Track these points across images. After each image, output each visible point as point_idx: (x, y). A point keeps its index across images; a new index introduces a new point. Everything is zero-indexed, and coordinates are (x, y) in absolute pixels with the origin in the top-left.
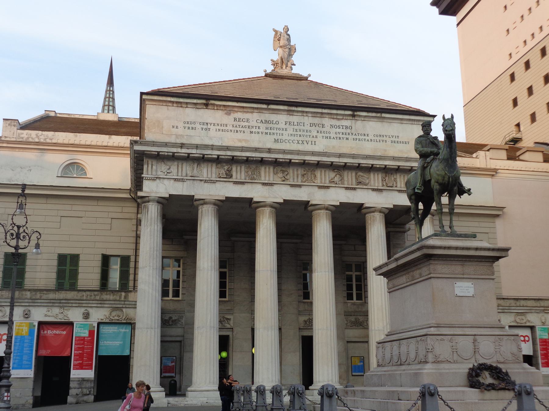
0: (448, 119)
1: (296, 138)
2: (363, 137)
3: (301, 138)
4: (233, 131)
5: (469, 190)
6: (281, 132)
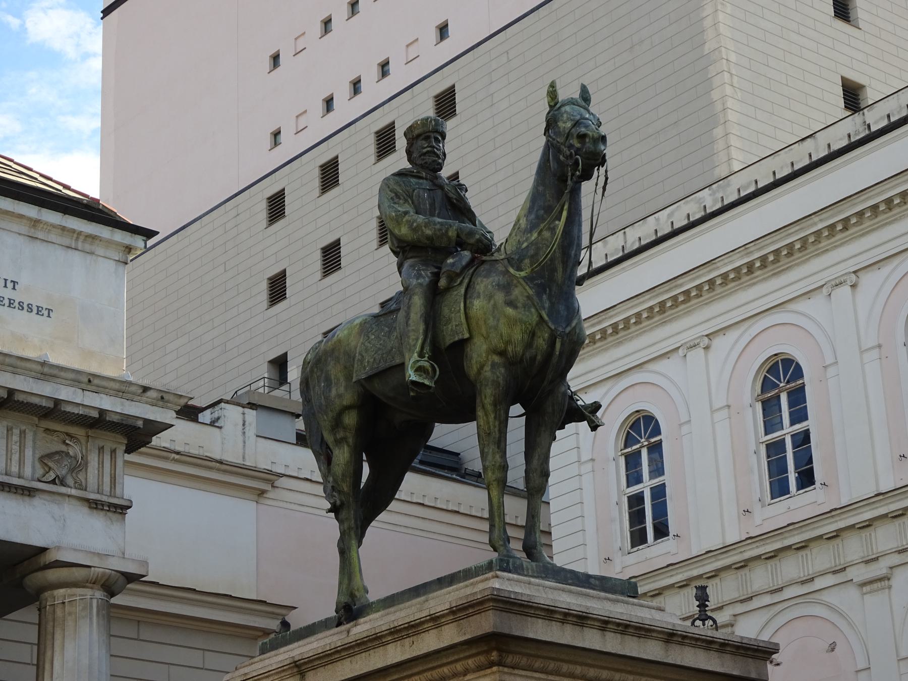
0: (572, 102)
5: (596, 406)
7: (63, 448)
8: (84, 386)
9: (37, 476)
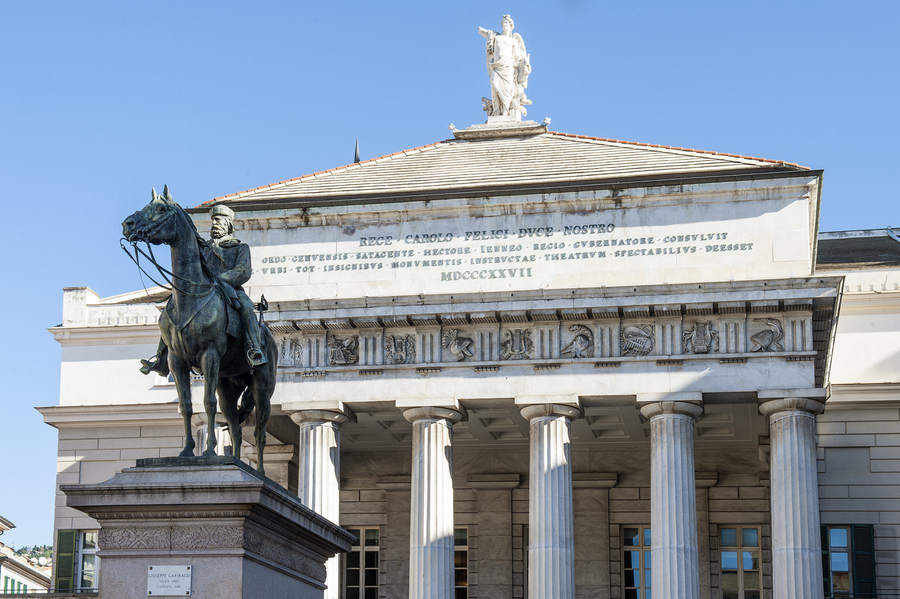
1: (488, 266)
2: (640, 246)
3: (501, 265)
4: (358, 267)
6: (456, 257)
7: (768, 328)
8: (763, 288)
9: (749, 349)
